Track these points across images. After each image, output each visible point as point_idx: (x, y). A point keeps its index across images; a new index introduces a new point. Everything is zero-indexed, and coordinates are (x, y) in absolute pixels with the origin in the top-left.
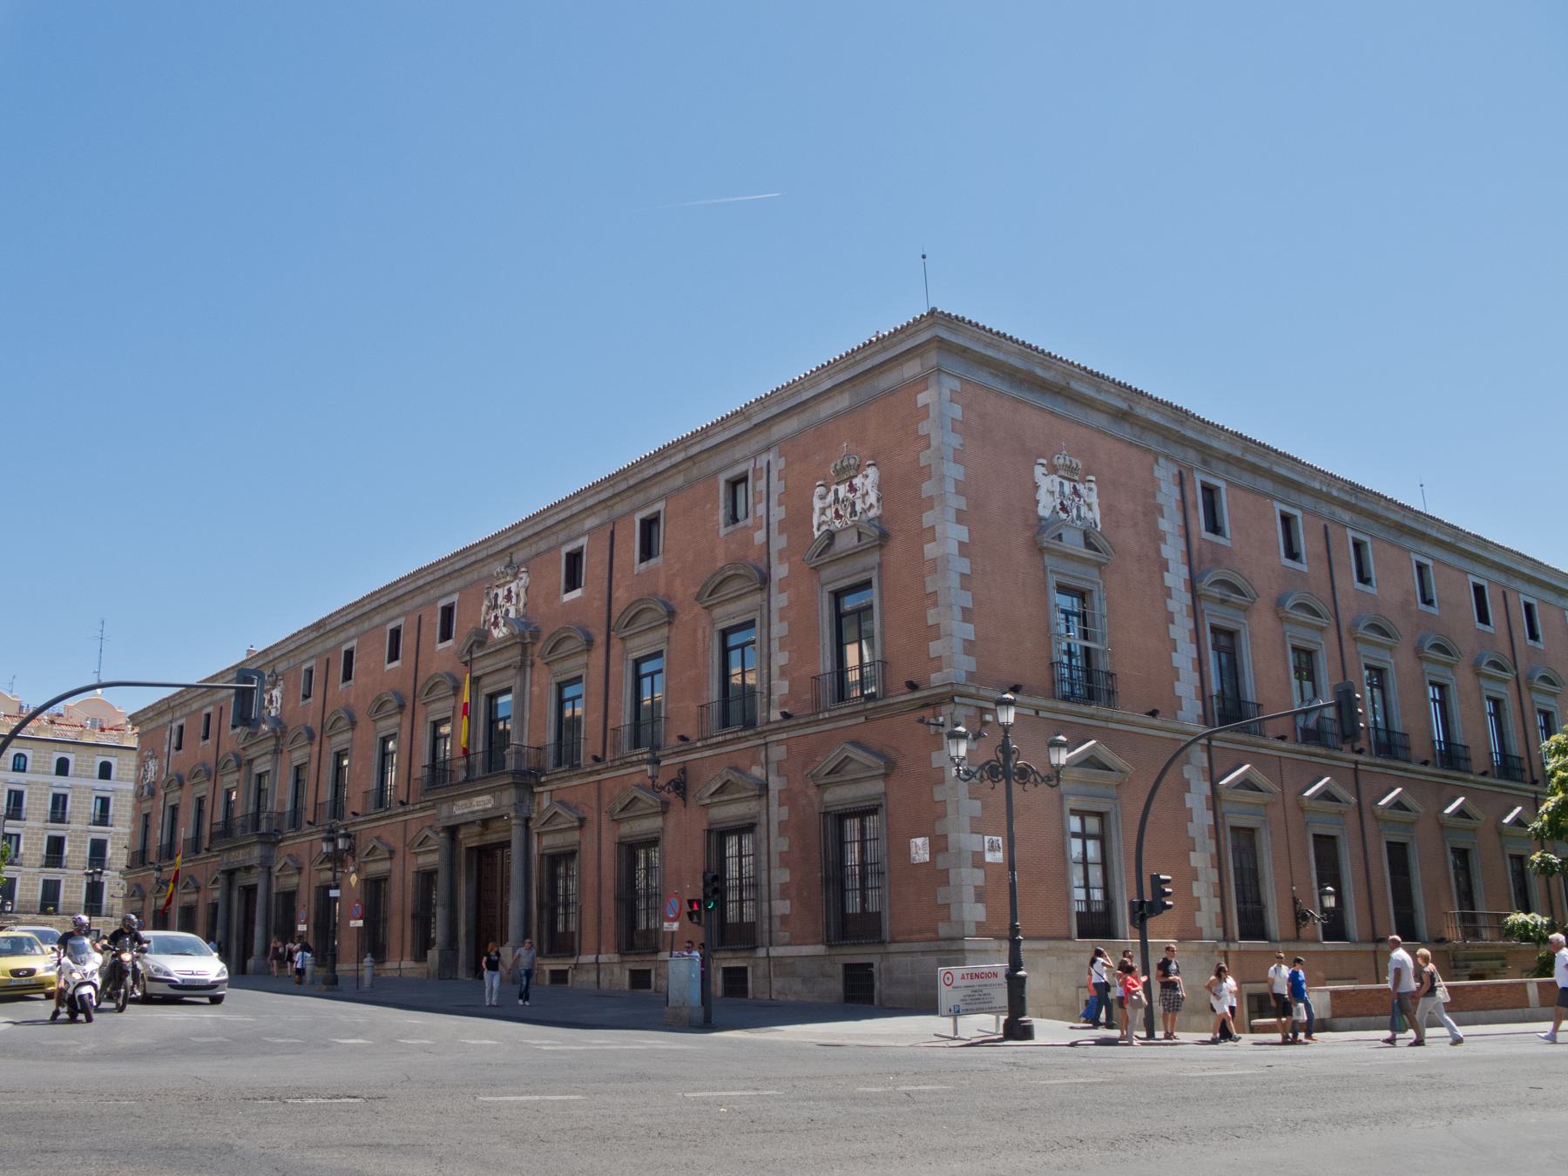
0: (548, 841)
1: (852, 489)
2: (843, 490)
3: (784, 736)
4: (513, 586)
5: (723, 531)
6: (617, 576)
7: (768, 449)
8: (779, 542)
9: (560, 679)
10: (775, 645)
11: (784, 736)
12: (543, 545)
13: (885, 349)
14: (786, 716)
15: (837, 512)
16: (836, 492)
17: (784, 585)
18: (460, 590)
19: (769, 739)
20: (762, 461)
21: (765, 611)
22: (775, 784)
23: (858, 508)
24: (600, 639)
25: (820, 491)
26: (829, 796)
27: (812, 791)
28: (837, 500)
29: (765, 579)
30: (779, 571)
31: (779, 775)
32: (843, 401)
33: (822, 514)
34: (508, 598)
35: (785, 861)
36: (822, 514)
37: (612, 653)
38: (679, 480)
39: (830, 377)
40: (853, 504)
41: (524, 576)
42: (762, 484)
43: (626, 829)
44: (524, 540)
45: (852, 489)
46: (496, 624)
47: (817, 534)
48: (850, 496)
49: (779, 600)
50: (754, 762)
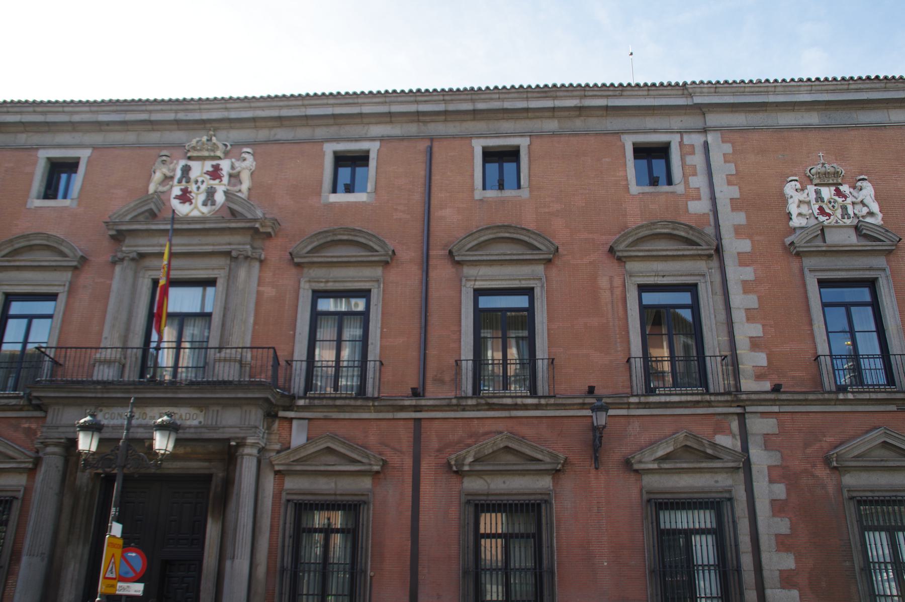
0: (290, 484)
1: (839, 193)
2: (827, 193)
3: (776, 409)
4: (225, 165)
5: (634, 189)
6: (438, 195)
7: (705, 131)
8: (730, 219)
9: (321, 286)
10: (738, 316)
11: (776, 409)
12: (303, 133)
13: (886, 89)
14: (776, 389)
15: (821, 209)
16: (818, 192)
17: (744, 260)
18: (95, 148)
19: (748, 409)
20: (696, 140)
21: (717, 278)
22: (760, 458)
23: (850, 211)
24: (409, 254)
25: (799, 186)
26: (849, 480)
27: (822, 472)
28: (819, 198)
29: (719, 250)
30: (734, 245)
31: (767, 448)
32: (813, 118)
33: (800, 203)
34: (215, 173)
35: (783, 543)
36: (800, 203)
37: (433, 274)
38: (552, 125)
39: (810, 92)
40: (844, 208)
41: (250, 158)
42: (697, 160)
43: (474, 485)
44: (254, 119)
45: (839, 193)
46: (185, 197)
47: (796, 222)
48: (840, 200)
49: (737, 274)
50: (720, 429)
